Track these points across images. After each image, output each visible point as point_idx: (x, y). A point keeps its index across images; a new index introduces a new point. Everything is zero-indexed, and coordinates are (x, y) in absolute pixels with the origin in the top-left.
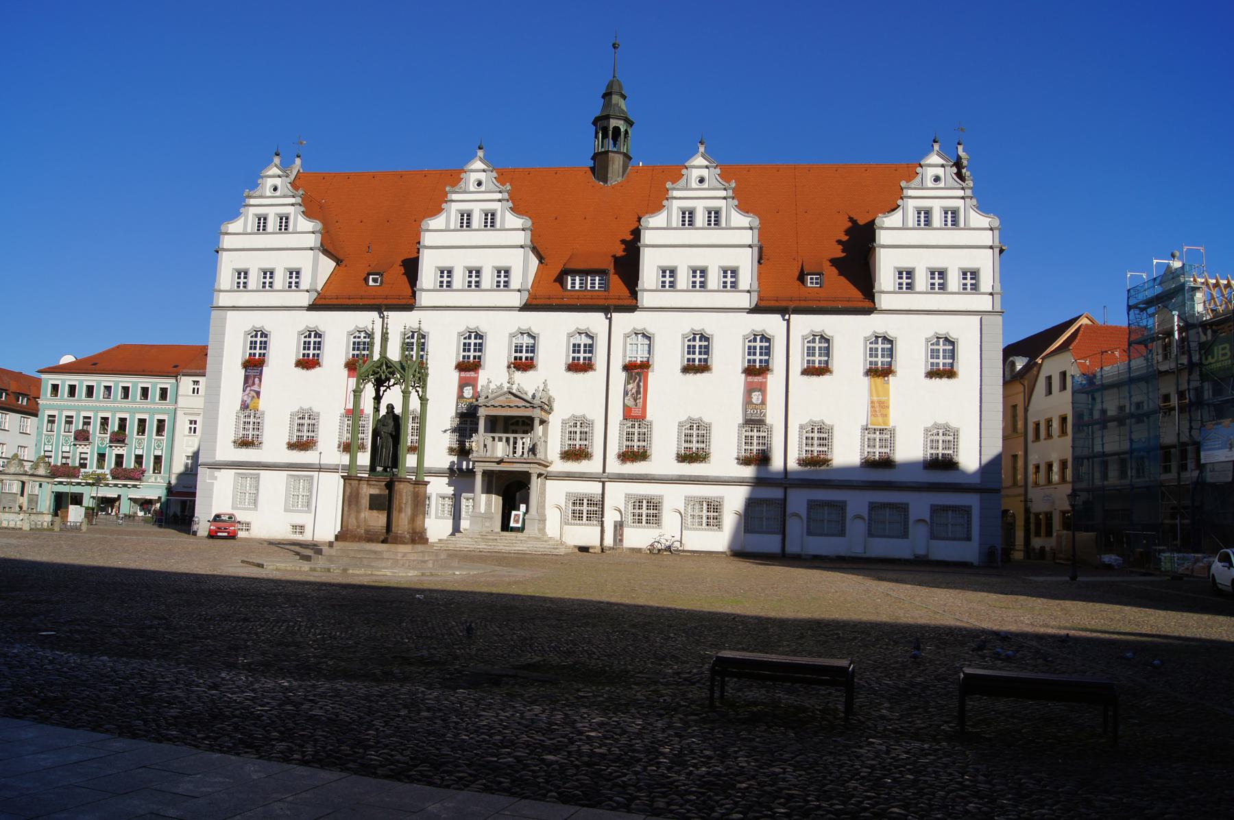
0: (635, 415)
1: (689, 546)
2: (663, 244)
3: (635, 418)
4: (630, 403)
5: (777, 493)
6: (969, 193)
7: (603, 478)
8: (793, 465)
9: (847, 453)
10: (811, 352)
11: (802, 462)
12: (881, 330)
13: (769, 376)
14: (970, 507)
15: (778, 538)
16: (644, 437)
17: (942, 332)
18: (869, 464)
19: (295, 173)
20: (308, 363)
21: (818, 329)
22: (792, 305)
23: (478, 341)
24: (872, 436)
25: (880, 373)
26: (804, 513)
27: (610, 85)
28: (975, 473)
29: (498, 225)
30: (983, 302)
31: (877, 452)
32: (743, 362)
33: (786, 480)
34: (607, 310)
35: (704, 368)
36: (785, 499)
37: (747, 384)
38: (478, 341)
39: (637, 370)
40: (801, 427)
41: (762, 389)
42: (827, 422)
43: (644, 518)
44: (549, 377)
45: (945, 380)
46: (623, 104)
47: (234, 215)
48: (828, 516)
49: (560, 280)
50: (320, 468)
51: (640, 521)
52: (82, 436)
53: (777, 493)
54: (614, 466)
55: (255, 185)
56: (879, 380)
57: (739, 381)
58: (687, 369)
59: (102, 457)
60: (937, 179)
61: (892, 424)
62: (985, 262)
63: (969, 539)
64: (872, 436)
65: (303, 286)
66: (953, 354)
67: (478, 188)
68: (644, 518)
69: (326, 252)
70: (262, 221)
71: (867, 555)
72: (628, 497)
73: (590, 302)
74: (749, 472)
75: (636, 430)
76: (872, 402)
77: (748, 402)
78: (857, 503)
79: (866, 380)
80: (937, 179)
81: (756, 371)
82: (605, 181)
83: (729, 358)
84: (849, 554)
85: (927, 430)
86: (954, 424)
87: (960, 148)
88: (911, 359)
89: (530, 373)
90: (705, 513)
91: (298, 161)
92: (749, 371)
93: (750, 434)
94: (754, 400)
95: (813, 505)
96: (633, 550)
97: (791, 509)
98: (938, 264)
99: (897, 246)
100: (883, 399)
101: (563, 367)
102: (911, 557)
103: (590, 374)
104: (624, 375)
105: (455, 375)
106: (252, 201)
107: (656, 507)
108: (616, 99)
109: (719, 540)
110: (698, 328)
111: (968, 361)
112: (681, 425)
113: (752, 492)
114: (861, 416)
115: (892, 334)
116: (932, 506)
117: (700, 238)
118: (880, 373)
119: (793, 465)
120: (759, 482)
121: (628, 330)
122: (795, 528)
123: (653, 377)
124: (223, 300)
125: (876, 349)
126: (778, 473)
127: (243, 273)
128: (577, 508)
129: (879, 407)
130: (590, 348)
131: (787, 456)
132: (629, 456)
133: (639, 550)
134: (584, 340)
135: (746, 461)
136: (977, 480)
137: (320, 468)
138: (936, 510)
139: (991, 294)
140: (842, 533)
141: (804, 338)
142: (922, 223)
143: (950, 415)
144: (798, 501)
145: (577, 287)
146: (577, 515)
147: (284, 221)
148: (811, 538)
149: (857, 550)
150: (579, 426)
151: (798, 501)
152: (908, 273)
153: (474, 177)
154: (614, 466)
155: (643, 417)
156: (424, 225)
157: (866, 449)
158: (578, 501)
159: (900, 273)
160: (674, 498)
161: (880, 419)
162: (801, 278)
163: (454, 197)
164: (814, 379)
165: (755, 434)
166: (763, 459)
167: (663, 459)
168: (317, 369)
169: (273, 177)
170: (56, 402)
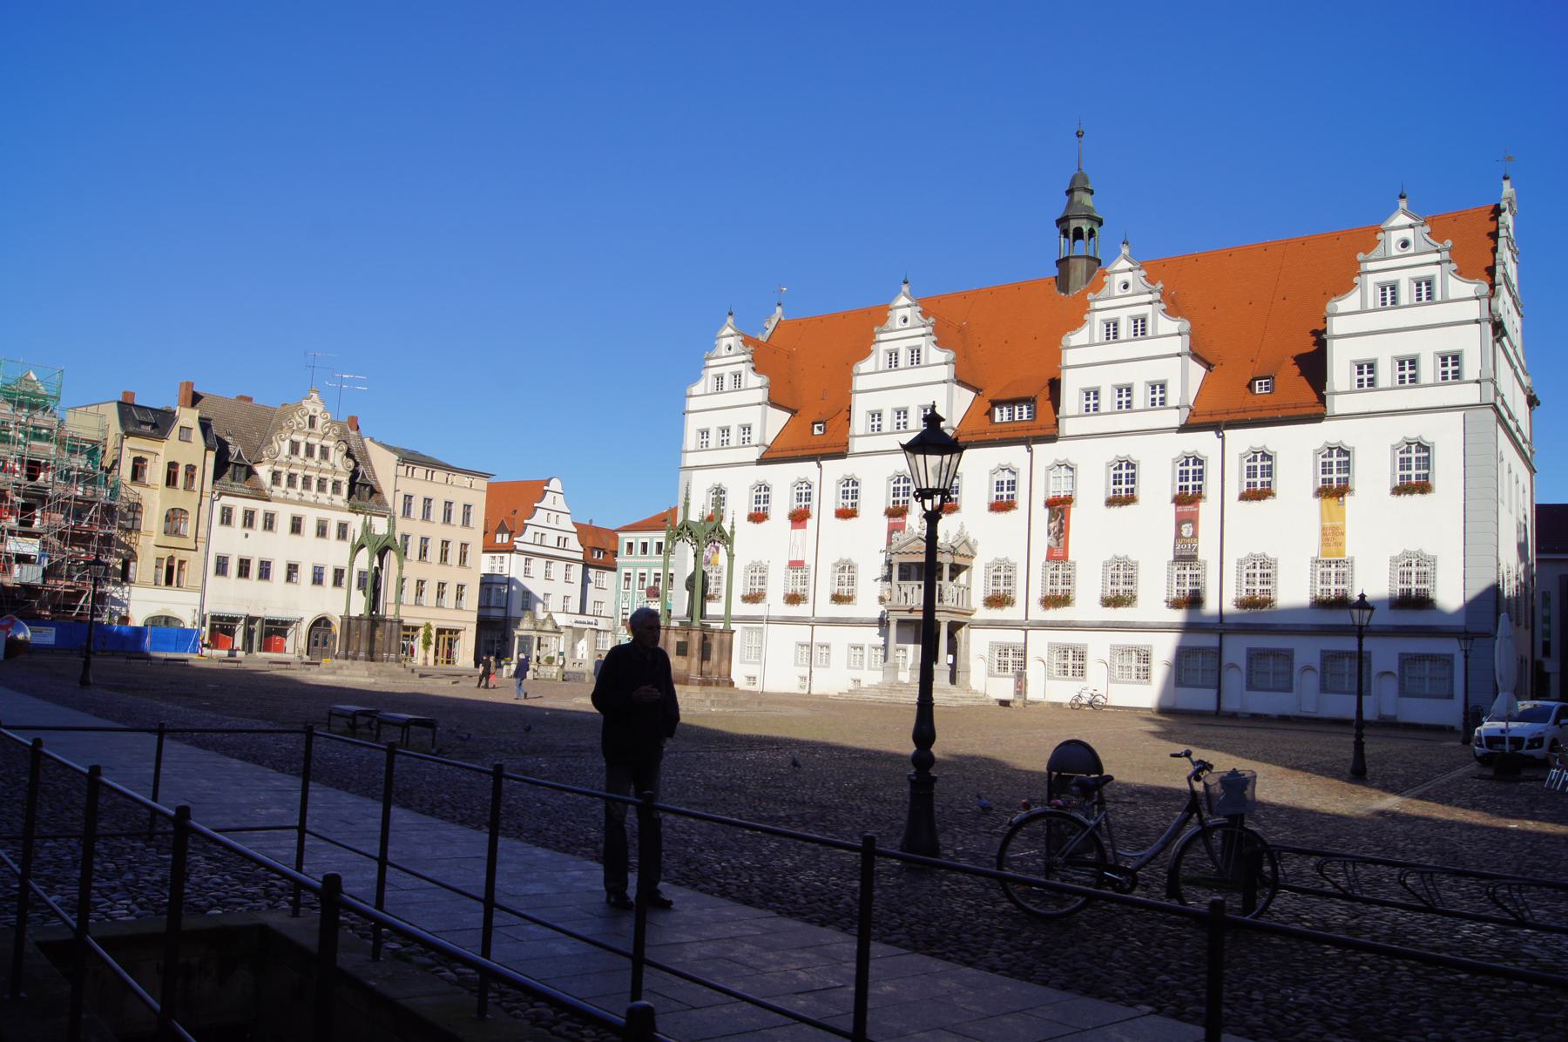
0: (1058, 555)
1: (1115, 701)
2: (1085, 362)
3: (1057, 559)
4: (1053, 544)
5: (1211, 641)
6: (1446, 255)
7: (1026, 626)
8: (1229, 607)
9: (1294, 591)
10: (1251, 472)
11: (1242, 604)
12: (1334, 440)
13: (1202, 504)
14: (1452, 656)
15: (1212, 693)
16: (1068, 580)
17: (1412, 435)
18: (1320, 604)
19: (774, 322)
20: (758, 517)
21: (1258, 445)
22: (1226, 418)
23: (1198, 467)
24: (1326, 570)
25: (1334, 491)
26: (1243, 664)
27: (1073, 181)
28: (1458, 612)
30: (1468, 394)
31: (1333, 589)
32: (1393, 478)
33: (1222, 626)
34: (1028, 441)
35: (1129, 499)
36: (1220, 648)
37: (1177, 515)
38: (1198, 467)
39: (1059, 507)
40: (1240, 562)
41: (1193, 520)
42: (1270, 555)
43: (1070, 669)
45: (1417, 497)
46: (1088, 200)
47: (696, 378)
48: (1269, 667)
49: (990, 414)
50: (769, 620)
51: (1065, 673)
53: (1211, 641)
54: (1038, 613)
55: (713, 347)
56: (1333, 502)
58: (1111, 502)
60: (1405, 244)
61: (1348, 554)
62: (1471, 342)
63: (1450, 696)
64: (1326, 570)
65: (753, 442)
66: (1426, 463)
67: (905, 326)
68: (1070, 669)
69: (961, 382)
70: (893, 356)
71: (1319, 715)
72: (993, 645)
73: (1012, 435)
74: (1178, 616)
75: (1060, 573)
76: (1324, 529)
77: (1178, 535)
78: (1307, 651)
79: (1317, 501)
81: (1187, 499)
82: (1067, 292)
83: (1157, 486)
84: (1297, 713)
85: (1394, 560)
86: (1429, 551)
87: (1506, 184)
88: (1374, 471)
90: (1134, 663)
91: (779, 310)
92: (1179, 500)
93: (1182, 572)
94: (1184, 533)
95: (1254, 656)
96: (1054, 704)
97: (1227, 658)
98: (1407, 351)
99: (1356, 331)
100: (1337, 523)
101: (986, 507)
102: (1375, 718)
104: (1047, 511)
105: (884, 522)
106: (711, 363)
107: (1082, 657)
108: (1077, 195)
109: (1147, 695)
110: (1123, 454)
111: (1447, 470)
112: (1106, 565)
113: (1182, 640)
114: (1313, 547)
115: (1348, 444)
116: (1401, 655)
117: (1128, 354)
118: (1334, 491)
119: (1229, 607)
120: (1188, 628)
121: (1050, 462)
122: (1234, 682)
123: (1075, 514)
124: (690, 460)
125: (1331, 464)
126: (1212, 617)
127: (705, 433)
129: (1332, 535)
130: (1012, 485)
131: (1222, 598)
132: (1050, 601)
133: (1059, 705)
134: (1006, 477)
135: (1175, 604)
136: (1461, 622)
137: (769, 620)
138: (1406, 660)
139: (1477, 382)
140: (1289, 689)
141: (1242, 456)
142: (1424, 296)
143: (1445, 543)
144: (1236, 650)
145: (1005, 419)
147: (916, 353)
148: (1252, 693)
149: (1309, 709)
150: (1002, 570)
151: (1236, 650)
152: (1162, 386)
153: (899, 314)
154: (1038, 613)
155: (1065, 558)
156: (1064, 341)
157: (1049, 587)
158: (1004, 650)
159: (1444, 359)
160: (1098, 646)
161: (1333, 549)
162: (1250, 386)
163: (882, 337)
164: (1255, 504)
165: (1188, 572)
166: (1194, 601)
167: (1086, 605)
168: (766, 523)
169: (728, 339)
170: (631, 560)
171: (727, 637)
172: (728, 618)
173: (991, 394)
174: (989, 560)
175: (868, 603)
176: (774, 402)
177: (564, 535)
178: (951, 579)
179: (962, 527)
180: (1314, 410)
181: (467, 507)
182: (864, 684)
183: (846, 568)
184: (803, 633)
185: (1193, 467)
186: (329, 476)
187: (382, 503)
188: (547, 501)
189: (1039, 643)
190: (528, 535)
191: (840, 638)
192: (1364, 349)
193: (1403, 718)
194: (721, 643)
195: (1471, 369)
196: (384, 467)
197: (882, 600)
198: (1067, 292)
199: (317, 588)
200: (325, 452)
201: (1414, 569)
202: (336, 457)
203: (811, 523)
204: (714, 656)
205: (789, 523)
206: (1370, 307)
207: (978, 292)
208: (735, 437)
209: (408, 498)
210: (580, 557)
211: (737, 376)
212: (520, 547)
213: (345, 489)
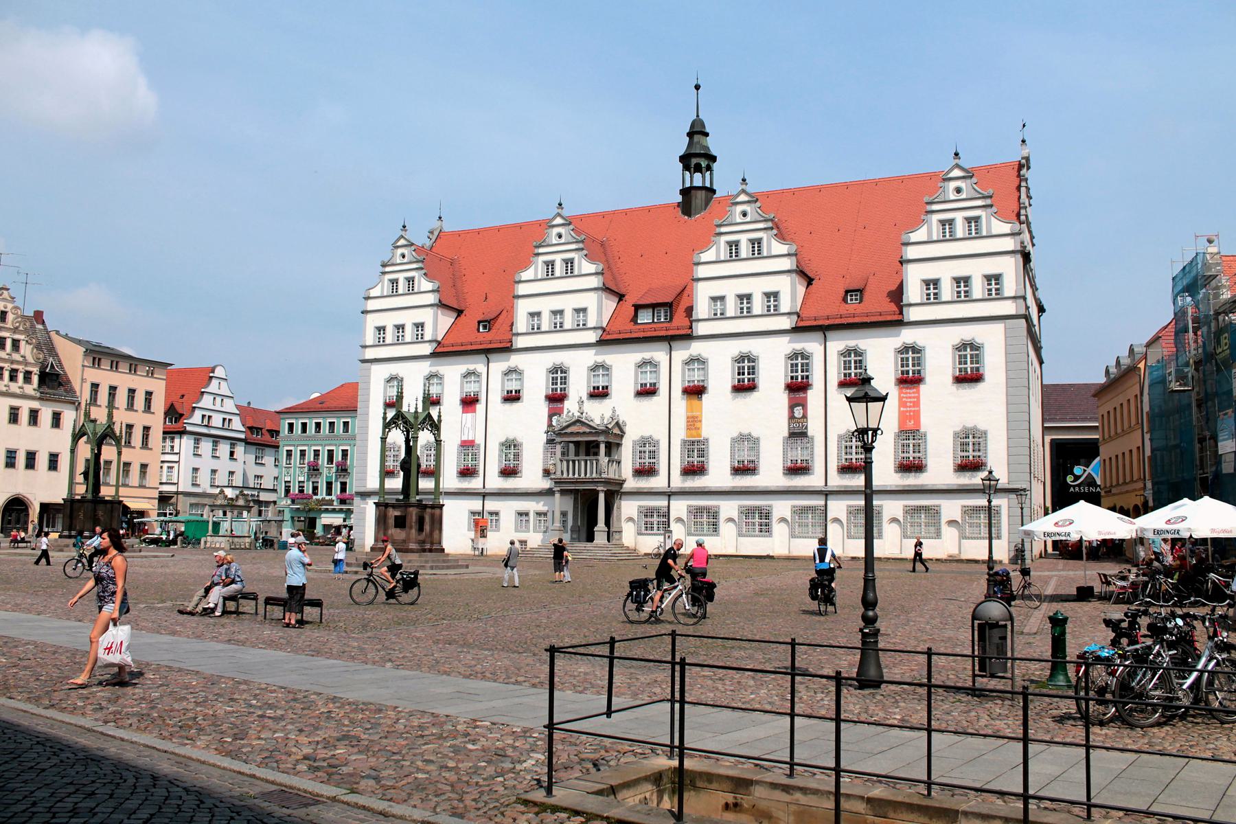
7: (669, 495)
10: (847, 365)
13: (809, 392)
29: (576, 273)
40: (840, 437)
41: (804, 405)
44: (623, 406)
52: (314, 469)
54: (678, 482)
57: (783, 398)
59: (329, 485)
62: (1009, 268)
77: (792, 417)
80: (958, 190)
81: (797, 388)
86: (982, 427)
89: (606, 401)
90: (757, 520)
94: (796, 415)
101: (632, 394)
103: (655, 398)
111: (994, 364)
125: (907, 359)
146: (649, 527)
150: (647, 445)
167: (719, 475)
171: (437, 511)
172: (437, 492)
173: (631, 300)
174: (636, 438)
175: (532, 477)
176: (442, 305)
177: (228, 417)
178: (608, 453)
179: (614, 411)
180: (896, 318)
181: (149, 394)
182: (530, 545)
183: (511, 446)
184: (476, 504)
185: (799, 360)
186: (20, 367)
187: (71, 391)
188: (213, 387)
189: (679, 507)
190: (197, 418)
191: (507, 509)
192: (930, 271)
193: (964, 556)
194: (432, 516)
195: (1010, 285)
196: (72, 361)
197: (547, 473)
198: (690, 216)
199: (10, 470)
200: (16, 344)
201: (971, 440)
202: (26, 350)
203: (480, 407)
204: (427, 527)
205: (460, 408)
206: (935, 238)
207: (614, 212)
208: (409, 334)
209: (95, 386)
210: (243, 436)
211: (410, 280)
212: (189, 428)
213: (35, 379)
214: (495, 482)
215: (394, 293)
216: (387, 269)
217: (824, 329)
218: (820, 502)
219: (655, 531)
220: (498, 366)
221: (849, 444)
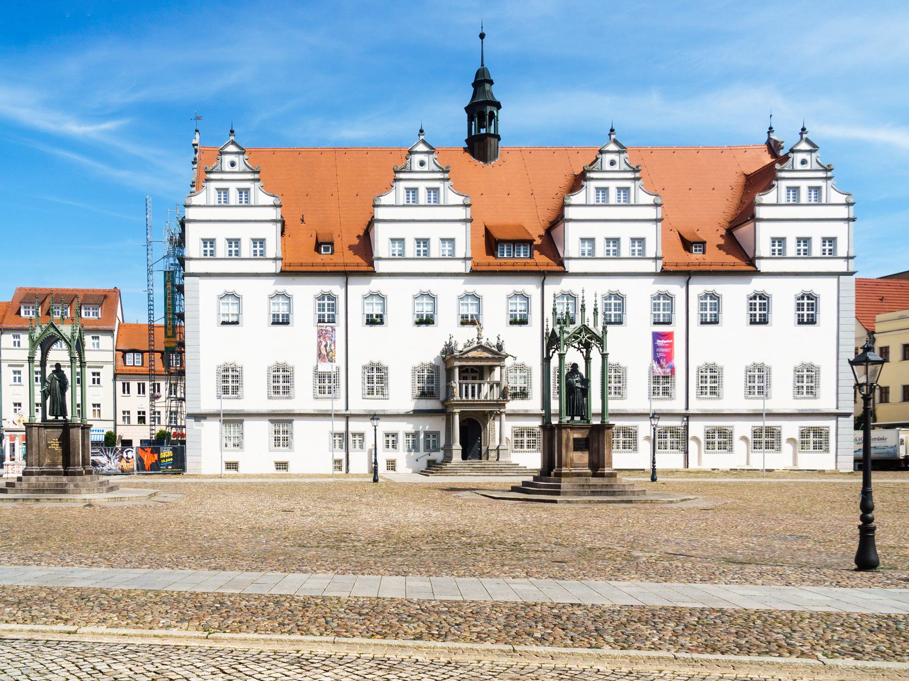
10: (703, 307)
40: (700, 370)
127: (209, 242)
128: (519, 439)
214: (358, 404)
215: (224, 204)
216: (212, 176)
217: (688, 274)
218: (677, 423)
219: (525, 449)
220: (358, 289)
221: (704, 374)
